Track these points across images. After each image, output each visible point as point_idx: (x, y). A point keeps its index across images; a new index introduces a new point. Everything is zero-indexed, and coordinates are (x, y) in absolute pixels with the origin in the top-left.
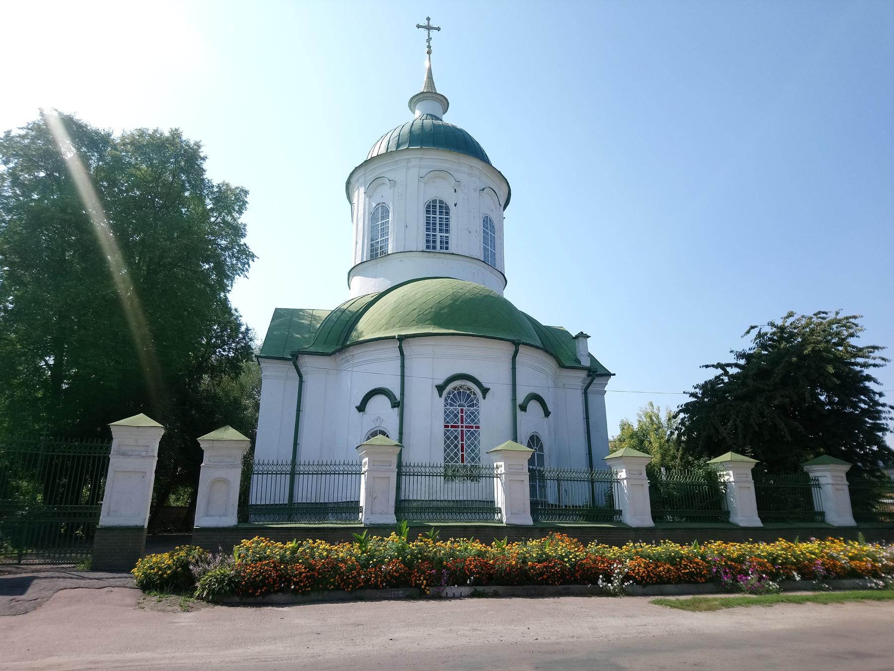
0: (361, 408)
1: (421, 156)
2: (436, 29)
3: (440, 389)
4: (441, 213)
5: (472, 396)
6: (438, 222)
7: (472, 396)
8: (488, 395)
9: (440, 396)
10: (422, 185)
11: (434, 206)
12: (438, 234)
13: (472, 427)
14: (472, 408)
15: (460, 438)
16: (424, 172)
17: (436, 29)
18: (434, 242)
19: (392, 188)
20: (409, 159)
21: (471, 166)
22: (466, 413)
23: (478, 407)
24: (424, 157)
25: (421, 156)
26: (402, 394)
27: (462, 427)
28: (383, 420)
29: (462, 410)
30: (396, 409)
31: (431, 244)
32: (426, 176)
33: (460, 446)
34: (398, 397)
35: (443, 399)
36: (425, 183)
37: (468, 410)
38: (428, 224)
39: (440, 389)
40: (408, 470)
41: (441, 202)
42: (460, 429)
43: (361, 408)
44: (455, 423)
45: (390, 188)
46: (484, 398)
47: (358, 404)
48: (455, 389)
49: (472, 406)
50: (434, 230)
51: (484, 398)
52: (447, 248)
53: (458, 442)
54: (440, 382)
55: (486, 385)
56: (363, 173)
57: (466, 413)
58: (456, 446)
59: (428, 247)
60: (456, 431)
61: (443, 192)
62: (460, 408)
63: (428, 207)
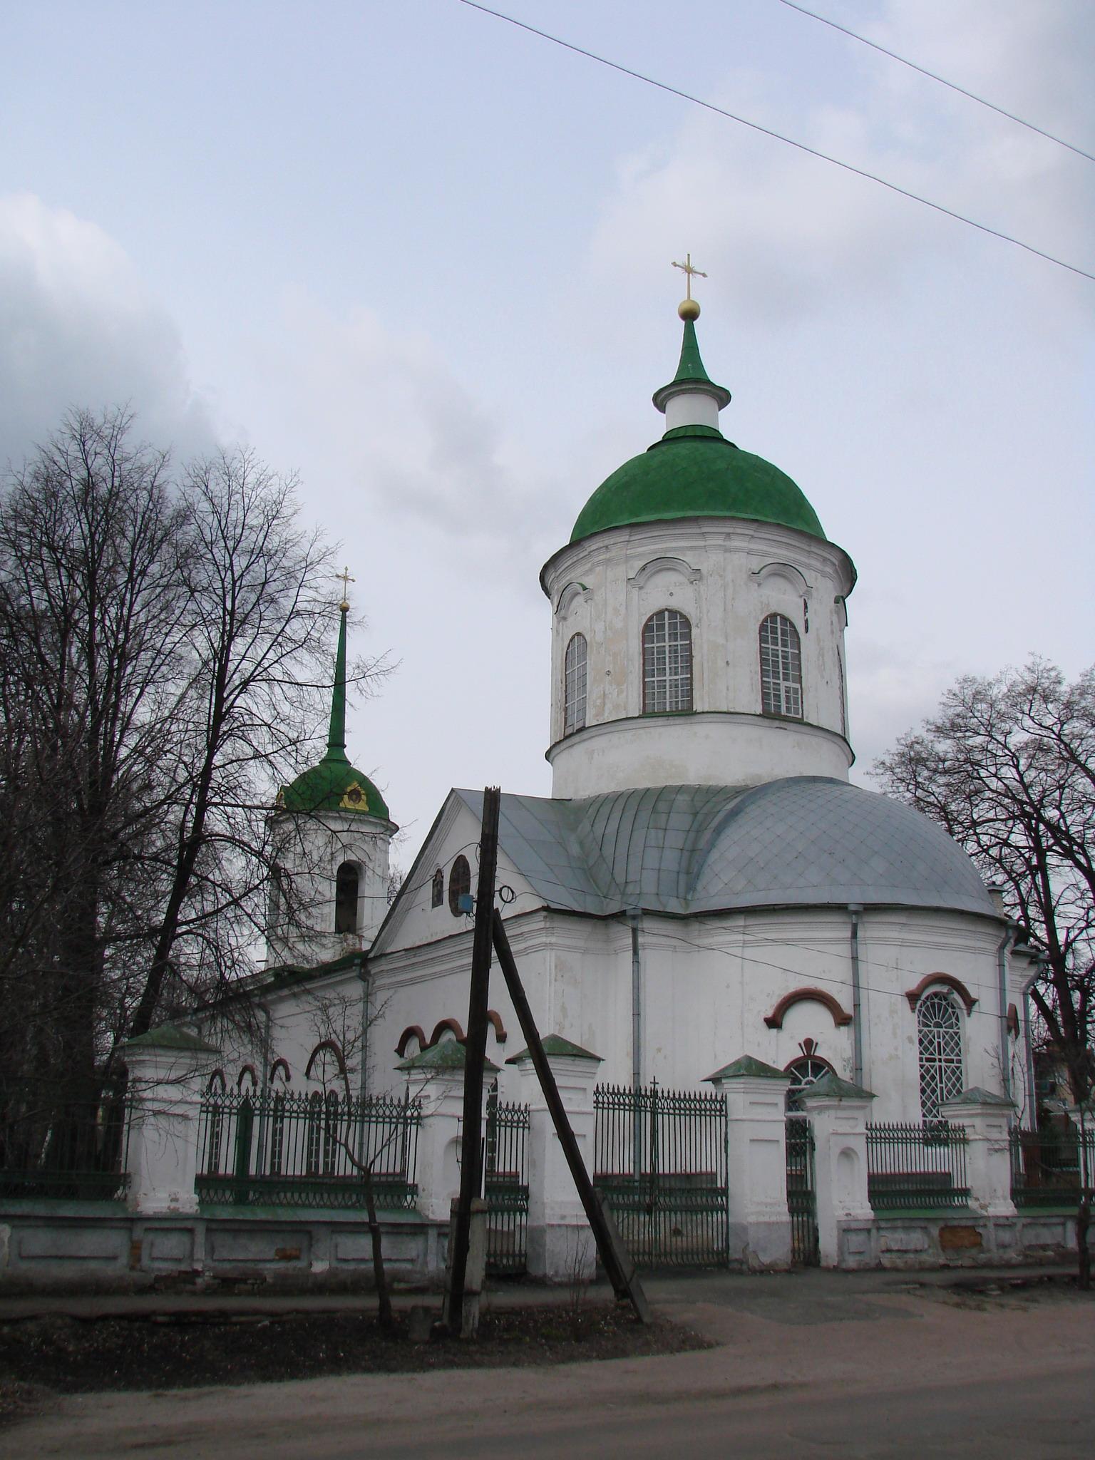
0: (774, 1022)
1: (751, 532)
3: (912, 997)
5: (950, 1010)
7: (950, 1010)
8: (975, 1008)
9: (913, 1010)
11: (774, 631)
12: (783, 685)
13: (952, 1061)
14: (951, 1031)
15: (938, 1077)
16: (755, 564)
18: (777, 697)
20: (728, 534)
21: (825, 559)
22: (944, 1037)
23: (958, 1029)
25: (751, 532)
26: (857, 1006)
27: (940, 1060)
28: (817, 1044)
29: (939, 1032)
30: (842, 1028)
32: (762, 572)
33: (938, 1091)
37: (947, 1033)
38: (763, 661)
39: (912, 997)
41: (785, 619)
42: (937, 1064)
43: (774, 1022)
44: (931, 1054)
46: (969, 1014)
47: (770, 1014)
48: (927, 998)
53: (936, 1086)
54: (913, 984)
55: (973, 995)
56: (627, 538)
57: (944, 1037)
58: (933, 1091)
60: (932, 1067)
61: (784, 599)
62: (936, 1030)
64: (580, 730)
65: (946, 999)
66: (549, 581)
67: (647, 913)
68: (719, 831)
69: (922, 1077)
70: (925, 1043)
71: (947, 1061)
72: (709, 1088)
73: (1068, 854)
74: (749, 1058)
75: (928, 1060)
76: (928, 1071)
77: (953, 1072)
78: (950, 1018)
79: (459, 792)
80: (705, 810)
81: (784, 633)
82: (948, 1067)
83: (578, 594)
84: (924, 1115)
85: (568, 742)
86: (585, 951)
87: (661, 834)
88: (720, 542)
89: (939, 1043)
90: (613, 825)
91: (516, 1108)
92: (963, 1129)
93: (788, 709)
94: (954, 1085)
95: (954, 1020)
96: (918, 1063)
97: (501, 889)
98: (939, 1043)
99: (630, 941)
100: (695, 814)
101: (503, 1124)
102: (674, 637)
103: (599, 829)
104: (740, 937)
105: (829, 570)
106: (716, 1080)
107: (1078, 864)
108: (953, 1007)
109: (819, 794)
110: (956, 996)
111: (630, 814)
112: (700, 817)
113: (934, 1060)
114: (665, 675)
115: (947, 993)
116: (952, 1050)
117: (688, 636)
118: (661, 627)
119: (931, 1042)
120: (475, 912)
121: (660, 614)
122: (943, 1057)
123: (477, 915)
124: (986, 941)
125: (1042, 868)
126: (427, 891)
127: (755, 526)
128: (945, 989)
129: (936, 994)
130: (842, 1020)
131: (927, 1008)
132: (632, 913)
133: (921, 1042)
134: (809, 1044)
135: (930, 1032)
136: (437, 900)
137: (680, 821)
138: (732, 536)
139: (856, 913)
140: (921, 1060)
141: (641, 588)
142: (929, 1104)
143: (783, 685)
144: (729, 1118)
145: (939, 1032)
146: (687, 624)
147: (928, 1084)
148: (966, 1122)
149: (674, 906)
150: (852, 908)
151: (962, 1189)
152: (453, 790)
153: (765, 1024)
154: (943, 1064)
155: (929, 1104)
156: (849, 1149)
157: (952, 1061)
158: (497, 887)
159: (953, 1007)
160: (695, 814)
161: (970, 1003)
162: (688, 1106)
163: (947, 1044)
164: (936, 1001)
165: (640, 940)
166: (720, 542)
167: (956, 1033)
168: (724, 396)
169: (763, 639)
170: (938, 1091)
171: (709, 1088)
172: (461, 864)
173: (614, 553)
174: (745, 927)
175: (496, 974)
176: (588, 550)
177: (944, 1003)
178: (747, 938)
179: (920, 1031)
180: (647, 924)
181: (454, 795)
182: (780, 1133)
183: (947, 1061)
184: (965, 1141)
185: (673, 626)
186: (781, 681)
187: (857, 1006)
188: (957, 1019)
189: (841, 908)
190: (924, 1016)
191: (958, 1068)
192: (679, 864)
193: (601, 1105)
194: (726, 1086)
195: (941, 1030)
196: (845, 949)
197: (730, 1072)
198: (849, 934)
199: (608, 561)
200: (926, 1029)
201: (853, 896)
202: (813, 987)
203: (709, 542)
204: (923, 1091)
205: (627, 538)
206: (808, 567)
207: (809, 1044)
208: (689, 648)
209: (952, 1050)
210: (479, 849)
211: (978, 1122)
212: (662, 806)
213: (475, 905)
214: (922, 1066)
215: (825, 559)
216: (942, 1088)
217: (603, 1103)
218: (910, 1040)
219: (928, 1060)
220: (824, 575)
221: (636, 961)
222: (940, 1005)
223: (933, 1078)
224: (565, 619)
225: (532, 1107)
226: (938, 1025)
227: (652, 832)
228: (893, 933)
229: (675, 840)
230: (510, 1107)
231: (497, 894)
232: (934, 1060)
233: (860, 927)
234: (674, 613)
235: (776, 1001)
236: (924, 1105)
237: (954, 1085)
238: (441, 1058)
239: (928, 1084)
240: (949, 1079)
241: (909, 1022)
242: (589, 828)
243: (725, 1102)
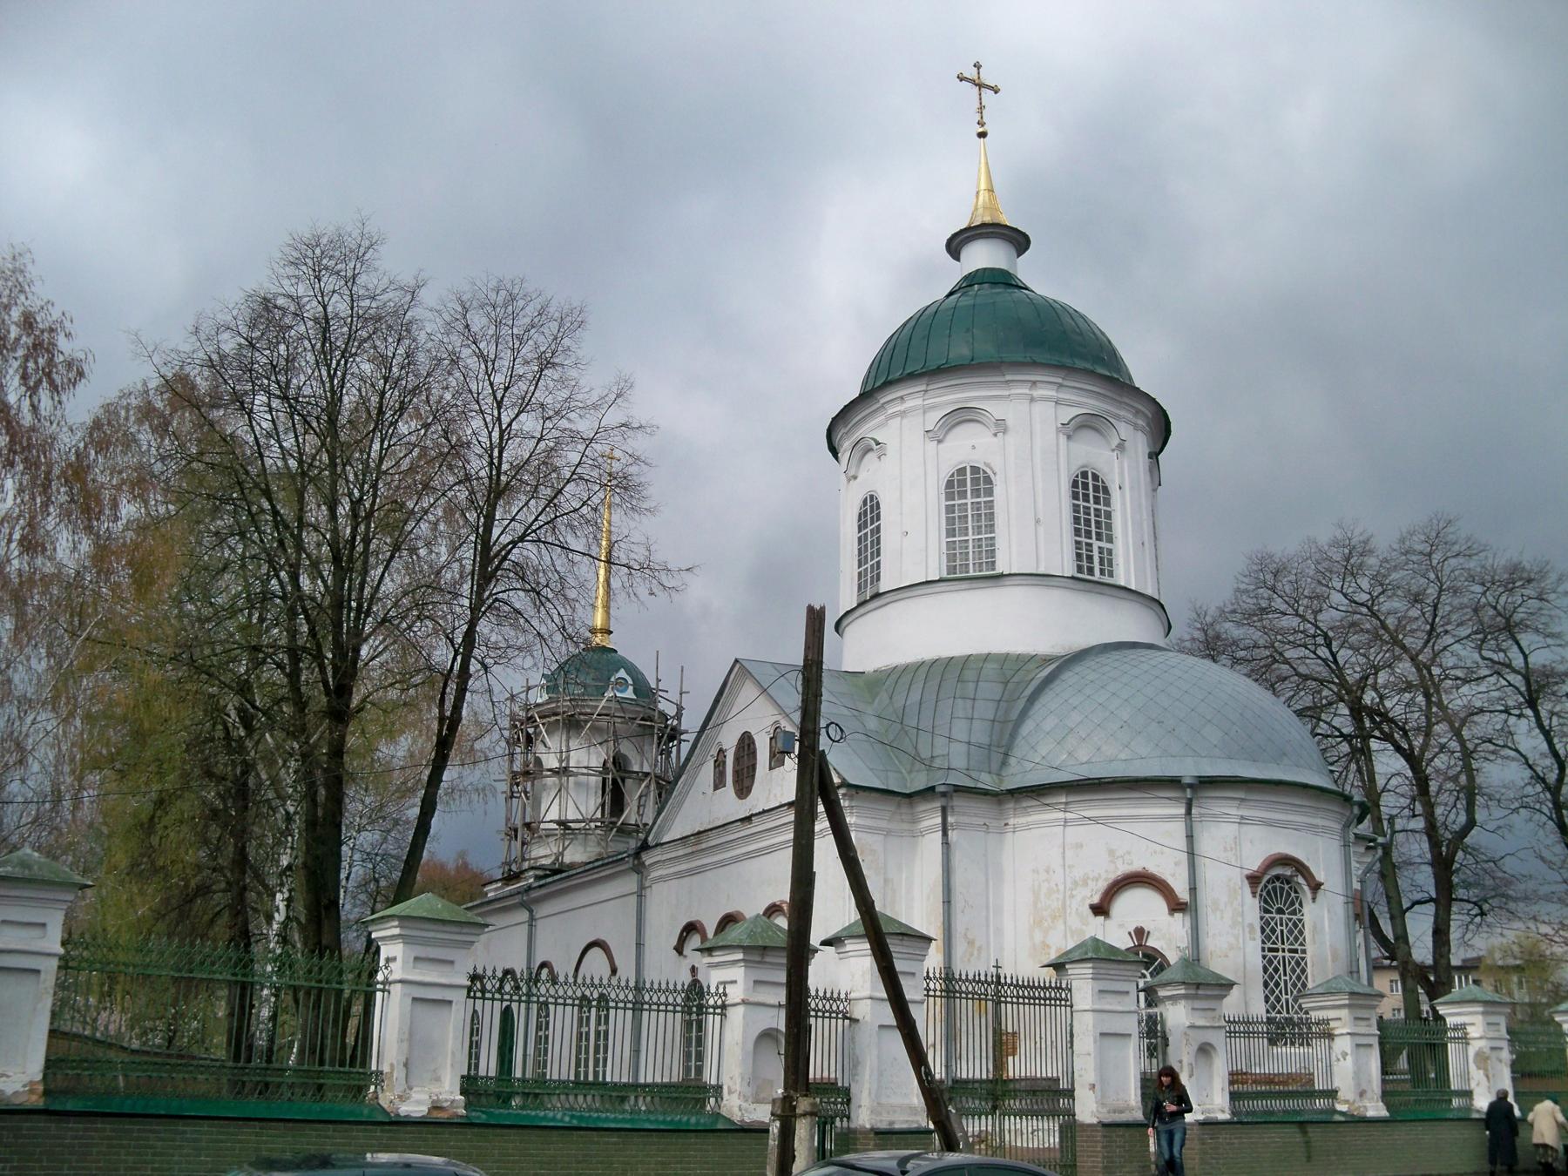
0: (1101, 910)
1: (1060, 380)
2: (966, 79)
3: (1253, 880)
4: (1097, 500)
5: (1293, 895)
6: (1093, 518)
7: (1293, 895)
8: (1320, 893)
9: (1254, 894)
10: (1063, 439)
11: (1085, 486)
12: (1096, 544)
13: (1295, 951)
14: (1294, 917)
15: (1281, 969)
16: (1067, 414)
17: (966, 79)
18: (1090, 558)
19: (1000, 435)
20: (1034, 383)
24: (1066, 383)
25: (1060, 380)
26: (1193, 890)
27: (1283, 950)
29: (1281, 919)
30: (1178, 916)
31: (1085, 564)
33: (1282, 984)
34: (1183, 894)
35: (1257, 901)
36: (1069, 437)
37: (1290, 920)
38: (1077, 520)
39: (1253, 880)
41: (1095, 477)
42: (1280, 954)
43: (1101, 910)
44: (1274, 943)
45: (995, 435)
46: (1314, 899)
47: (1096, 900)
48: (1268, 882)
49: (1294, 913)
50: (1088, 534)
51: (1314, 899)
52: (1111, 574)
54: (1254, 865)
58: (1277, 985)
59: (1080, 569)
60: (1275, 957)
62: (1278, 916)
63: (1075, 484)
64: (877, 596)
65: (1288, 883)
66: (836, 441)
67: (959, 789)
68: (1032, 699)
69: (1265, 970)
70: (1267, 930)
71: (1291, 951)
72: (1049, 975)
73: (1387, 738)
74: (1095, 940)
75: (1271, 950)
76: (1270, 962)
77: (1298, 964)
78: (1293, 904)
79: (746, 664)
80: (1015, 679)
81: (1096, 489)
82: (1293, 958)
83: (871, 449)
84: (1268, 1012)
85: (862, 610)
86: (888, 833)
87: (969, 703)
88: (1027, 391)
89: (1282, 931)
90: (915, 696)
91: (835, 996)
92: (1327, 1022)
93: (1102, 572)
94: (1299, 978)
95: (1297, 905)
96: (1260, 953)
97: (828, 726)
98: (1282, 931)
99: (939, 820)
100: (1006, 683)
101: (820, 1014)
102: (976, 493)
103: (899, 701)
104: (1061, 815)
105: (1140, 422)
106: (1058, 966)
107: (1398, 749)
108: (1296, 892)
109: (1143, 659)
110: (1300, 880)
111: (933, 684)
112: (1010, 686)
113: (1277, 950)
114: (967, 535)
115: (1291, 876)
116: (1296, 939)
117: (990, 492)
118: (962, 483)
119: (1273, 931)
120: (797, 752)
121: (962, 471)
122: (1286, 946)
123: (799, 756)
124: (1328, 821)
125: (1366, 752)
126: (708, 771)
127: (1063, 373)
128: (1288, 872)
129: (1277, 877)
130: (1176, 906)
131: (1268, 893)
132: (942, 789)
133: (1263, 930)
134: (1140, 933)
135: (1272, 919)
136: (719, 783)
137: (991, 690)
138: (1039, 385)
139: (1191, 786)
140: (1263, 950)
141: (940, 442)
142: (1272, 999)
143: (1096, 544)
144: (1075, 1008)
145: (1281, 919)
146: (988, 480)
147: (1271, 977)
148: (1331, 1014)
149: (986, 781)
150: (1187, 781)
151: (1328, 1091)
152: (737, 661)
153: (1090, 911)
154: (1287, 954)
155: (1272, 999)
156: (1210, 1045)
157: (1295, 951)
158: (823, 723)
159: (1296, 892)
160: (1006, 683)
161: (1316, 887)
162: (1032, 993)
163: (1291, 932)
164: (1278, 884)
165: (950, 819)
166: (1027, 391)
167: (1300, 921)
168: (1021, 239)
169: (1075, 496)
170: (1282, 984)
171: (1049, 975)
172: (746, 744)
173: (909, 404)
174: (1066, 803)
175: (822, 824)
176: (882, 401)
177: (1286, 887)
178: (1069, 815)
179: (1262, 918)
180: (958, 802)
181: (738, 666)
182: (1131, 1025)
183: (1291, 951)
184: (1330, 1036)
185: (975, 481)
186: (1093, 541)
187: (1193, 890)
188: (1301, 905)
189: (1173, 783)
190: (1266, 902)
191: (1303, 959)
192: (991, 736)
193: (931, 993)
194: (1070, 972)
195: (1284, 917)
196: (1179, 828)
197: (1076, 956)
198: (1182, 811)
199: (903, 414)
200: (1267, 916)
201: (1188, 769)
202: (1140, 869)
203: (1013, 391)
204: (1266, 985)
205: (923, 387)
206: (1118, 417)
207: (1140, 933)
208: (990, 505)
209: (1296, 939)
210: (800, 676)
211: (1344, 1013)
212: (970, 674)
213: (797, 744)
214: (1264, 957)
215: (1137, 412)
216: (1286, 981)
217: (935, 991)
218: (1251, 926)
219: (1271, 950)
220: (1136, 427)
221: (946, 843)
222: (1282, 889)
223: (1276, 970)
224: (855, 478)
225: (853, 996)
226: (1280, 911)
227: (959, 702)
228: (1233, 810)
229: (986, 710)
230: (828, 995)
231: (823, 732)
232: (1277, 950)
233: (1195, 803)
234: (975, 470)
235: (1102, 885)
236: (1267, 999)
237: (1299, 978)
238: (749, 936)
239: (1271, 977)
240: (1294, 971)
241: (1251, 907)
242: (888, 701)
243: (1070, 990)
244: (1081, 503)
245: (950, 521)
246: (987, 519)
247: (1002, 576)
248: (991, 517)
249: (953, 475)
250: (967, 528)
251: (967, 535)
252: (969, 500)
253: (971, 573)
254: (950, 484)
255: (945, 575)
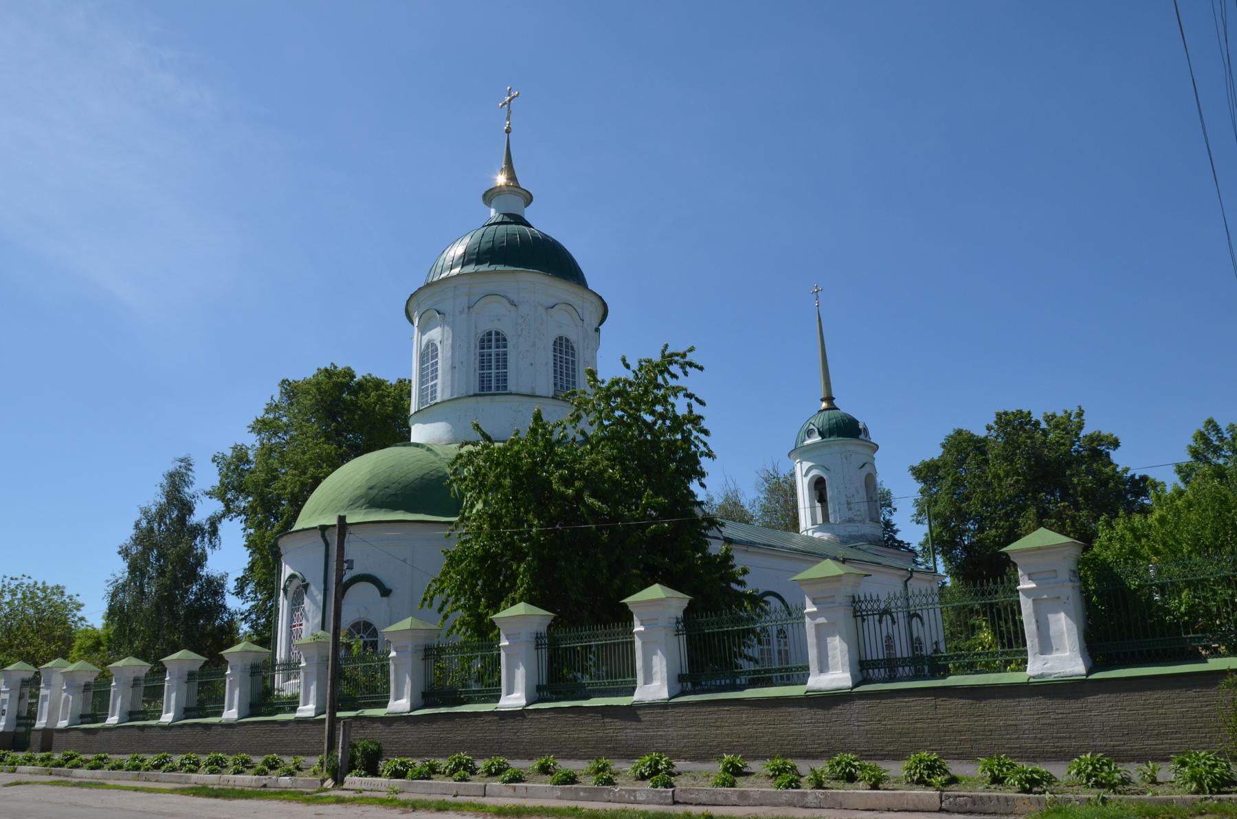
40: (869, 607)
114: (491, 369)
118: (490, 341)
121: (490, 334)
146: (505, 340)
185: (497, 340)
208: (505, 354)
234: (497, 333)
244: (570, 358)
245: (482, 362)
246: (503, 361)
247: (511, 394)
248: (505, 360)
249: (484, 335)
250: (491, 366)
251: (491, 369)
252: (493, 351)
253: (493, 391)
254: (482, 341)
255: (477, 392)
